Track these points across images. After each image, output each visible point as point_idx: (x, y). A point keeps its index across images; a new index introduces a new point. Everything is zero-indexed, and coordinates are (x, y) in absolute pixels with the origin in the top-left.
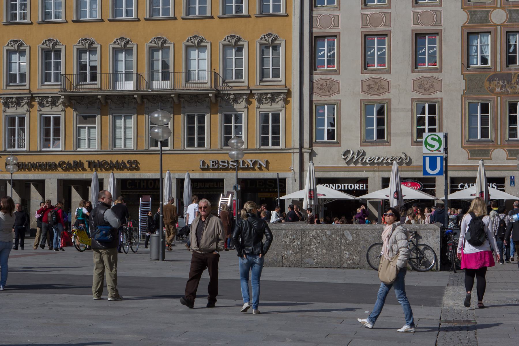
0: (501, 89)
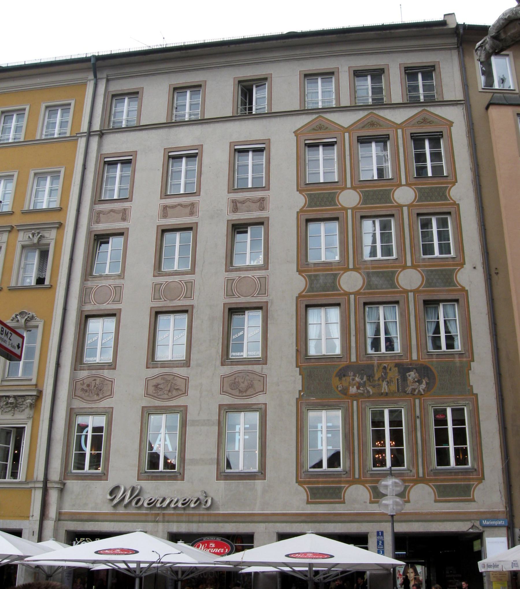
0: (358, 388)
